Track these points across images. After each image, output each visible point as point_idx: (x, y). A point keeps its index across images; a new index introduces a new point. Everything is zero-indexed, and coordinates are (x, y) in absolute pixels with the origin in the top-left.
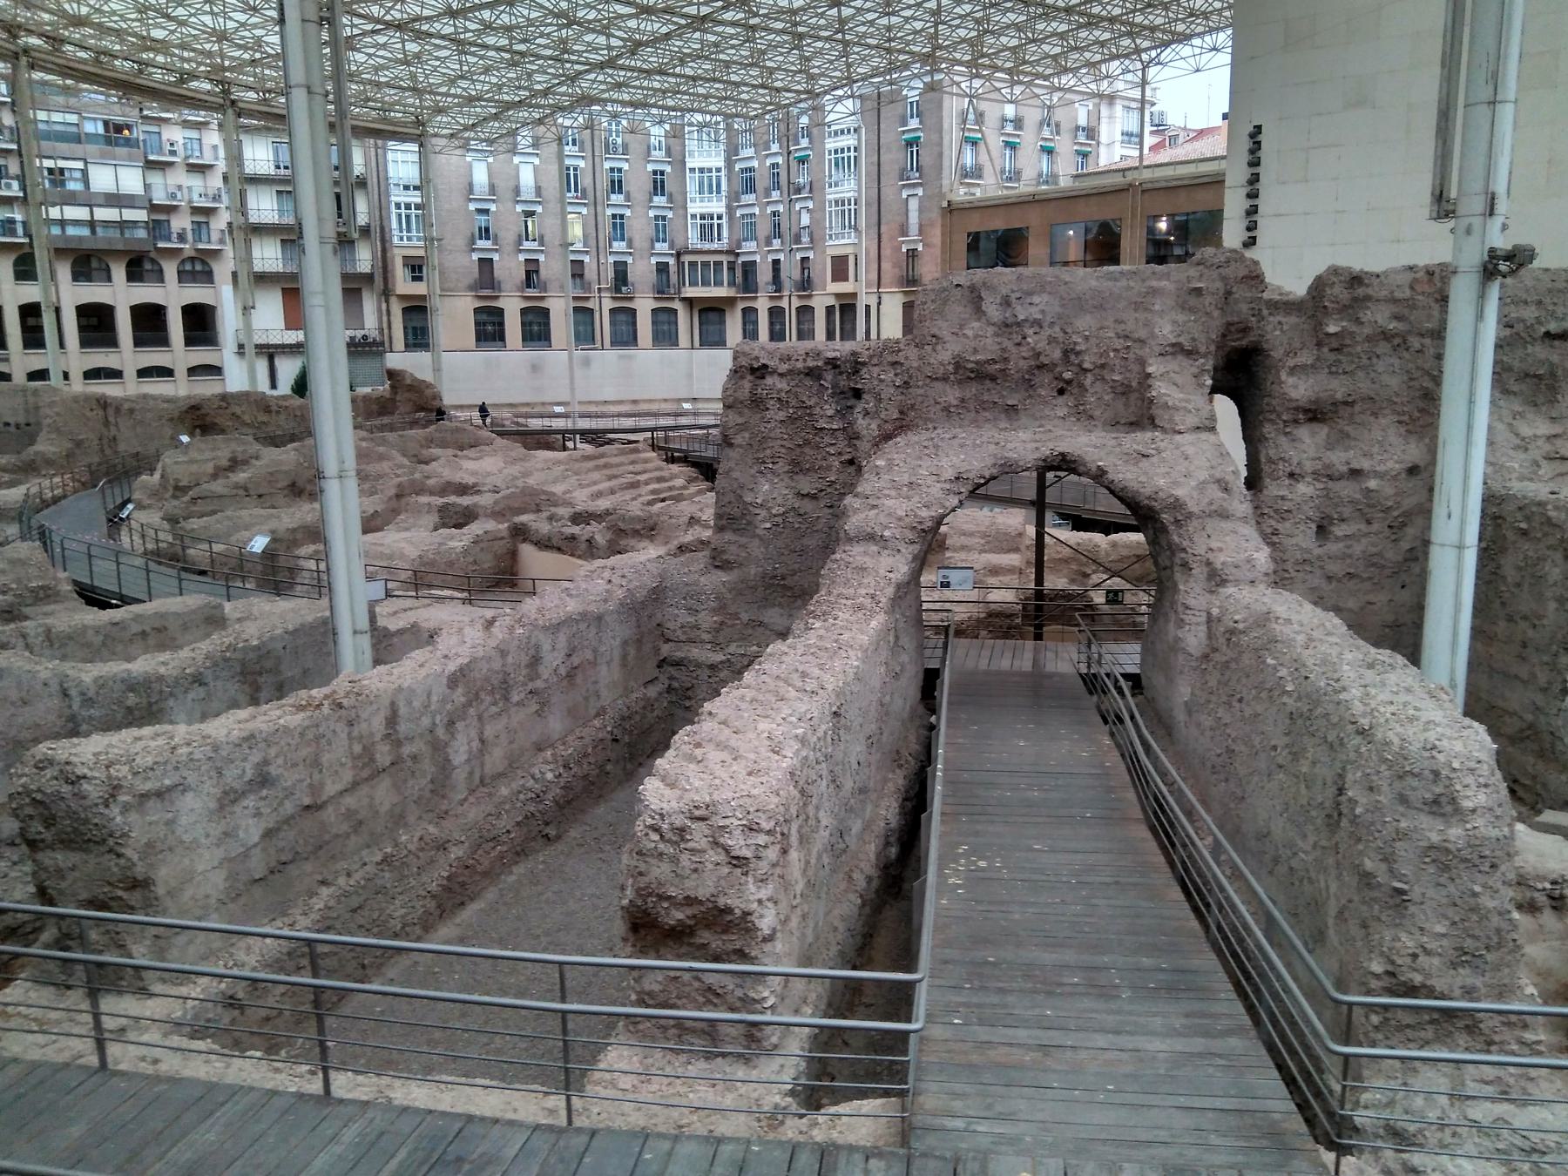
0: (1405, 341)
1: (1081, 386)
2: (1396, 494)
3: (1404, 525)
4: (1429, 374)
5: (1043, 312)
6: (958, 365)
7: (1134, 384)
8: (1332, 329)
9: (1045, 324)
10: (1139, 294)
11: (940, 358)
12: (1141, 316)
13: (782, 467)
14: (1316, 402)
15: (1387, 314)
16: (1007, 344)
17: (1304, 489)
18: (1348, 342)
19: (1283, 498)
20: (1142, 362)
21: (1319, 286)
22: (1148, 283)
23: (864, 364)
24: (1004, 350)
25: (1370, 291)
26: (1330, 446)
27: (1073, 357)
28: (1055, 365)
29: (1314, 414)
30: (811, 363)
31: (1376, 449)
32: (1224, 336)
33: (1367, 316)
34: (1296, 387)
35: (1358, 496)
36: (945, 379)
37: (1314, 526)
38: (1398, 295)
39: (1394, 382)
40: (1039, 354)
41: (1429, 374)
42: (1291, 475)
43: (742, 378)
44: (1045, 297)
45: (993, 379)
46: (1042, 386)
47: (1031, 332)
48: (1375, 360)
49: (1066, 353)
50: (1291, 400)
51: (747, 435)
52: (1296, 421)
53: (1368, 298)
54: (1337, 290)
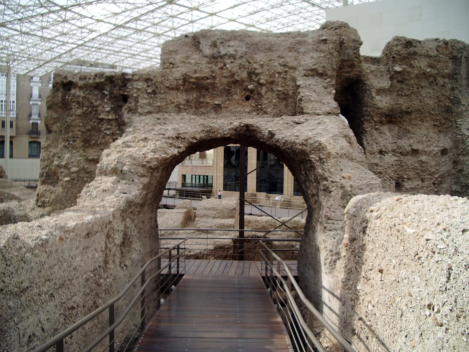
0: (435, 80)
1: (259, 94)
2: (436, 165)
3: (441, 183)
4: (448, 98)
5: (236, 51)
6: (185, 79)
7: (290, 93)
8: (398, 68)
9: (237, 57)
10: (291, 43)
11: (174, 76)
12: (292, 54)
13: (79, 143)
14: (392, 110)
15: (426, 63)
16: (216, 68)
17: (389, 159)
18: (406, 77)
19: (377, 165)
20: (294, 80)
21: (389, 47)
22: (296, 39)
23: (129, 80)
24: (213, 72)
25: (416, 49)
26: (400, 137)
27: (254, 77)
28: (243, 81)
29: (392, 118)
30: (98, 80)
31: (424, 139)
32: (340, 68)
33: (416, 63)
34: (381, 101)
35: (417, 165)
36: (177, 89)
37: (394, 182)
38: (431, 53)
39: (431, 102)
40: (234, 74)
41: (448, 98)
42: (381, 152)
43: (58, 90)
44: (237, 43)
45: (207, 89)
46: (236, 94)
47: (228, 61)
48: (420, 89)
49: (250, 74)
50: (378, 108)
51: (59, 124)
52: (381, 122)
53: (415, 53)
54: (399, 48)
